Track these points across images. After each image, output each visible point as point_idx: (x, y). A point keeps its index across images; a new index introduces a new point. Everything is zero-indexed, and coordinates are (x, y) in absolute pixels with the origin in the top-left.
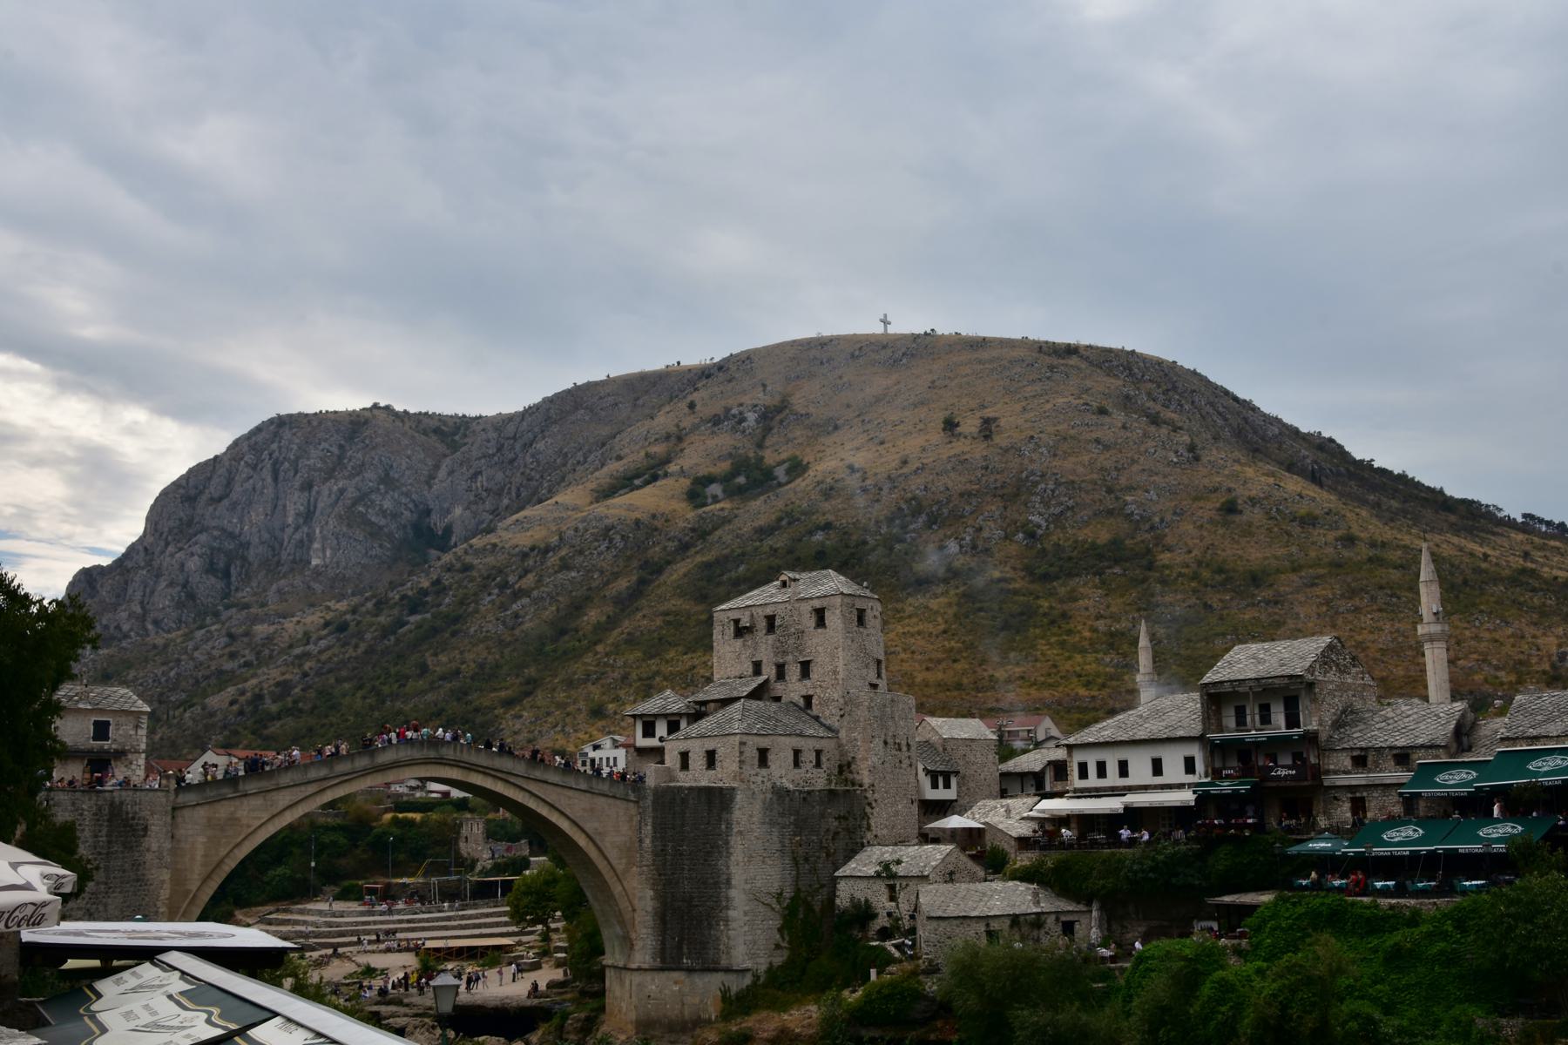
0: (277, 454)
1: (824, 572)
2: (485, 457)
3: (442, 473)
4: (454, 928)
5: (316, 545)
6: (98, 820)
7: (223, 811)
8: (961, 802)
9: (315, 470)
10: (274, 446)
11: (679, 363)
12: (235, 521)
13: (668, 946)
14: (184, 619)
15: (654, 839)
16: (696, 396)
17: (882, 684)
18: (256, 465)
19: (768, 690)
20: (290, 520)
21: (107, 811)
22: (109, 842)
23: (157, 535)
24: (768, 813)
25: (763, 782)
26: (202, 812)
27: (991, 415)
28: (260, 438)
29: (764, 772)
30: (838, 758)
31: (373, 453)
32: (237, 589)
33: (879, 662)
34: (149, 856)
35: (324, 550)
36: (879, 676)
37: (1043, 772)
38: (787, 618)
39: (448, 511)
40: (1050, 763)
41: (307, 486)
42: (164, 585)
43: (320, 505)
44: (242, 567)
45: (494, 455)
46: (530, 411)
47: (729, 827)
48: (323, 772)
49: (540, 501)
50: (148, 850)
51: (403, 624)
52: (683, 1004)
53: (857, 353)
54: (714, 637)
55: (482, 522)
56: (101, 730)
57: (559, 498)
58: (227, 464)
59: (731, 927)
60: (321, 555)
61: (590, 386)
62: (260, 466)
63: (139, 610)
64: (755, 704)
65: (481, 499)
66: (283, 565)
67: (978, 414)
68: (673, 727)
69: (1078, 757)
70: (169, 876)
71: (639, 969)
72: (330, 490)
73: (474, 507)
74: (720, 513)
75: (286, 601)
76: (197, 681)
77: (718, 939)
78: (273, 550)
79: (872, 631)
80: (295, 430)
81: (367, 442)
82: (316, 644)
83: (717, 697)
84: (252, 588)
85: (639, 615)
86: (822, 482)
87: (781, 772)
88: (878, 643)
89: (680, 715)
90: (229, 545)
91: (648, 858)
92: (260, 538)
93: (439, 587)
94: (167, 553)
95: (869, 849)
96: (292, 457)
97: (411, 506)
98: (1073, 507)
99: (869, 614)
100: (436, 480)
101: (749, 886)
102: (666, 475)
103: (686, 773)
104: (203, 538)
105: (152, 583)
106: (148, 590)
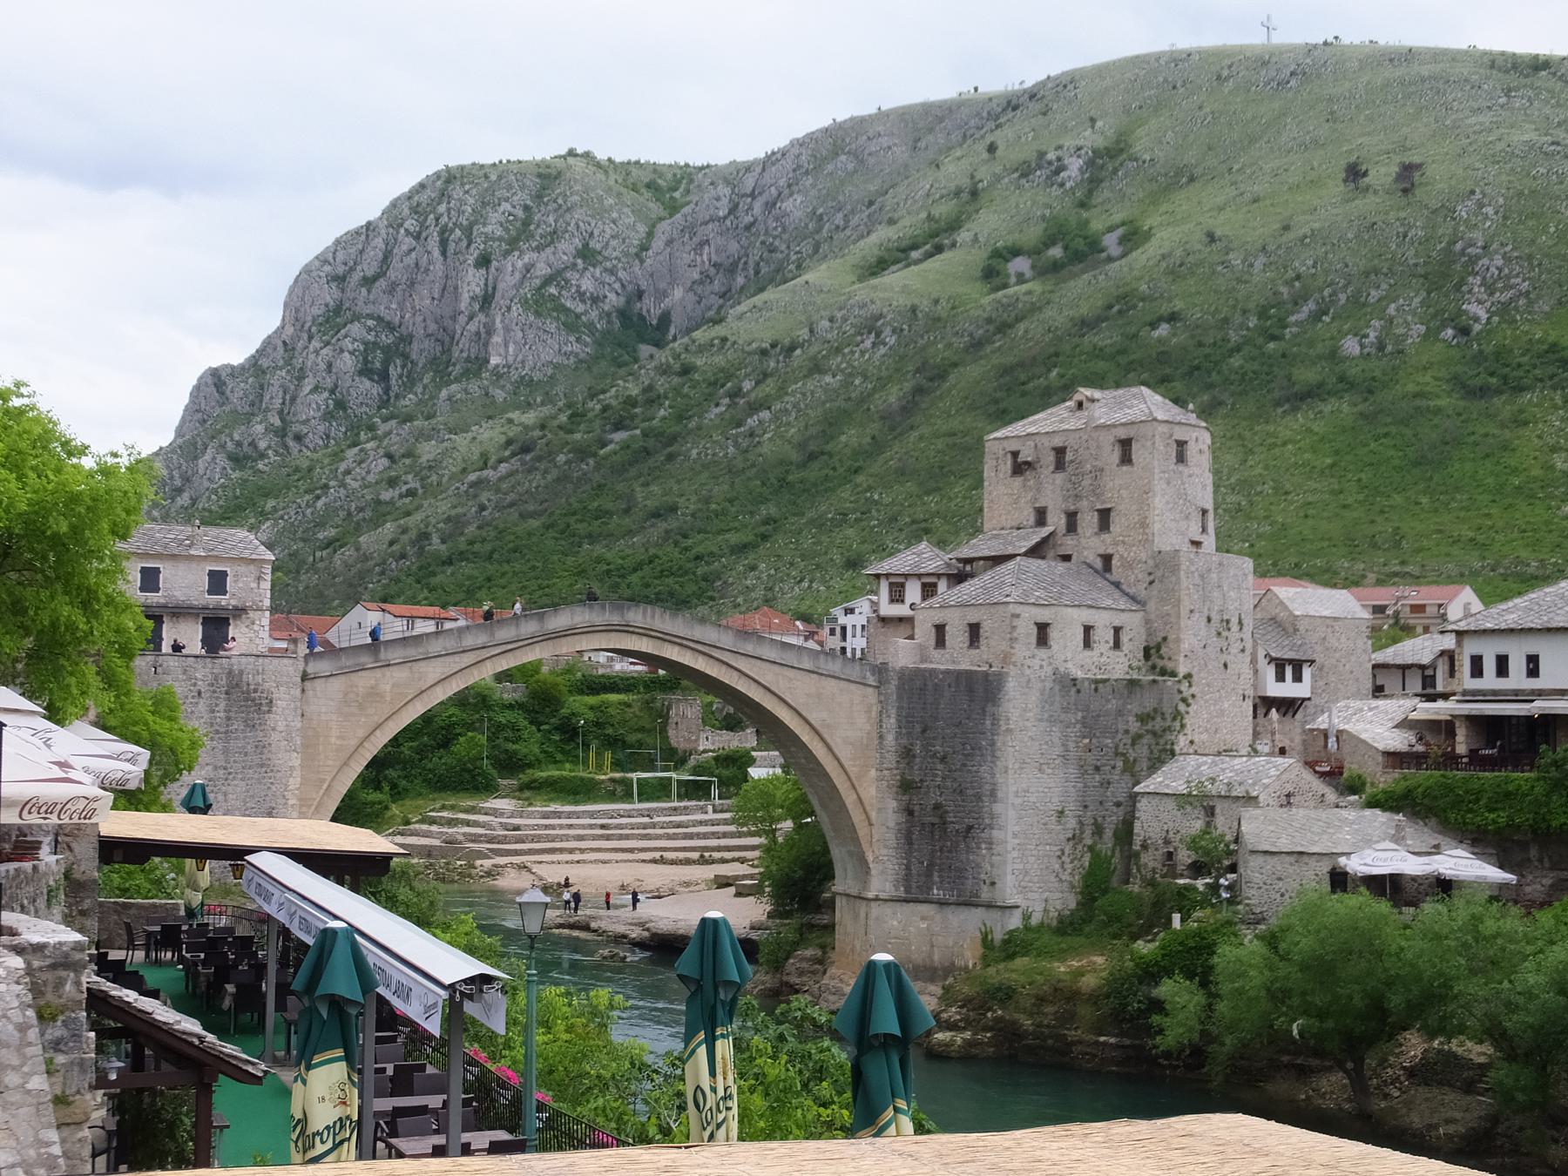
0: (445, 219)
1: (1134, 390)
2: (712, 220)
3: (658, 244)
4: (658, 837)
5: (497, 339)
6: (214, 692)
7: (363, 681)
8: (1315, 701)
9: (493, 240)
10: (442, 208)
11: (976, 89)
12: (394, 306)
13: (914, 872)
14: (332, 434)
15: (898, 735)
16: (999, 137)
17: (1209, 542)
18: (419, 233)
19: (1054, 546)
20: (463, 306)
21: (224, 682)
22: (228, 718)
23: (298, 327)
24: (1047, 706)
25: (1041, 667)
26: (336, 685)
27: (1416, 159)
28: (424, 198)
29: (1043, 653)
30: (1144, 637)
31: (568, 216)
32: (397, 396)
33: (1204, 512)
34: (275, 736)
35: (506, 346)
36: (1204, 530)
37: (1433, 665)
38: (1081, 451)
39: (665, 294)
40: (1443, 653)
41: (484, 261)
42: (307, 389)
43: (501, 286)
44: (403, 367)
46: (771, 160)
47: (995, 720)
48: (482, 639)
49: (785, 282)
50: (274, 729)
52: (932, 946)
53: (1225, 73)
54: (985, 475)
55: (710, 308)
56: (217, 582)
57: (809, 276)
58: (383, 232)
59: (995, 852)
60: (502, 351)
61: (857, 126)
62: (424, 235)
63: (278, 423)
64: (1034, 564)
65: (707, 276)
66: (454, 365)
67: (1397, 159)
68: (929, 590)
69: (1471, 647)
70: (299, 762)
71: (877, 899)
72: (513, 265)
73: (699, 289)
74: (1027, 298)
75: (459, 411)
76: (349, 514)
77: (979, 866)
78: (443, 343)
79: (1196, 471)
80: (467, 187)
81: (560, 201)
82: (495, 468)
83: (987, 553)
84: (416, 394)
85: (915, 434)
86: (1170, 254)
87: (1068, 654)
88: (1204, 486)
89: (939, 576)
90: (387, 339)
91: (891, 759)
92: (425, 328)
93: (652, 398)
94: (311, 348)
95: (1182, 758)
96: (465, 223)
97: (617, 286)
98: (1528, 292)
99: (1191, 451)
100: (650, 252)
101: (1020, 801)
102: (954, 245)
103: (942, 652)
104: (355, 329)
105: (292, 387)
106: (288, 397)
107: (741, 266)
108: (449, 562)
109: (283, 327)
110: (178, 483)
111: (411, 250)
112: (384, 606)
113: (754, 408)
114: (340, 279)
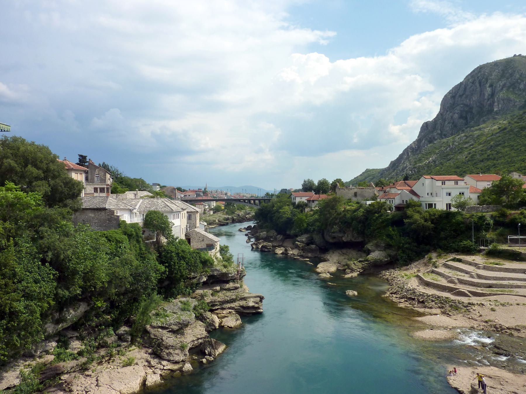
0: (480, 78)
5: (496, 104)
12: (468, 101)
20: (486, 97)
28: (474, 73)
32: (470, 122)
35: (498, 105)
41: (491, 86)
43: (496, 91)
63: (439, 132)
72: (499, 85)
90: (466, 109)
92: (476, 105)
104: (458, 108)
108: (482, 161)
109: (440, 110)
112: (432, 177)
114: (453, 97)
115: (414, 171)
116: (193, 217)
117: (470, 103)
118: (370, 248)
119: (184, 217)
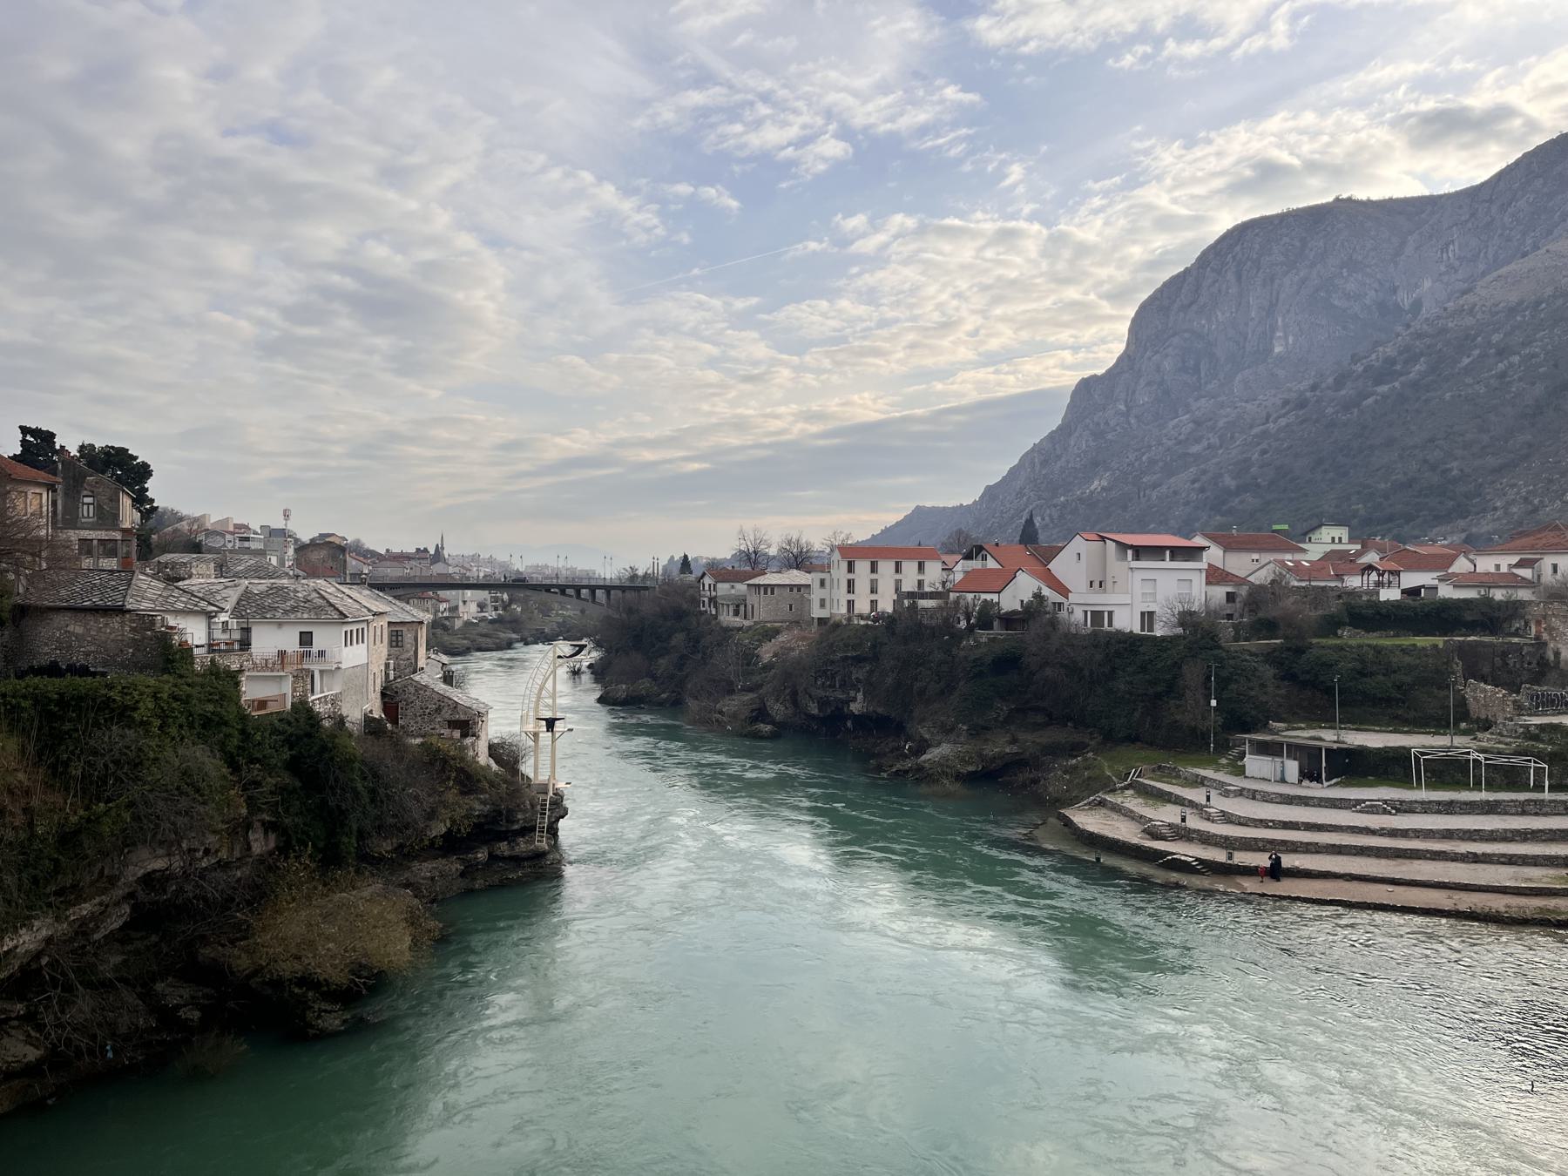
2: (1456, 224)
12: (1203, 322)
20: (1253, 315)
32: (1206, 383)
35: (1286, 338)
39: (1417, 286)
43: (1282, 296)
45: (1467, 221)
51: (1364, 396)
63: (1122, 407)
65: (1453, 268)
73: (1445, 279)
82: (1275, 422)
97: (1376, 285)
100: (1403, 257)
104: (1176, 340)
107: (1482, 255)
110: (1058, 452)
111: (1215, 282)
113: (1502, 352)
115: (1050, 516)
116: (408, 637)
117: (1209, 329)
118: (927, 736)
119: (378, 639)
